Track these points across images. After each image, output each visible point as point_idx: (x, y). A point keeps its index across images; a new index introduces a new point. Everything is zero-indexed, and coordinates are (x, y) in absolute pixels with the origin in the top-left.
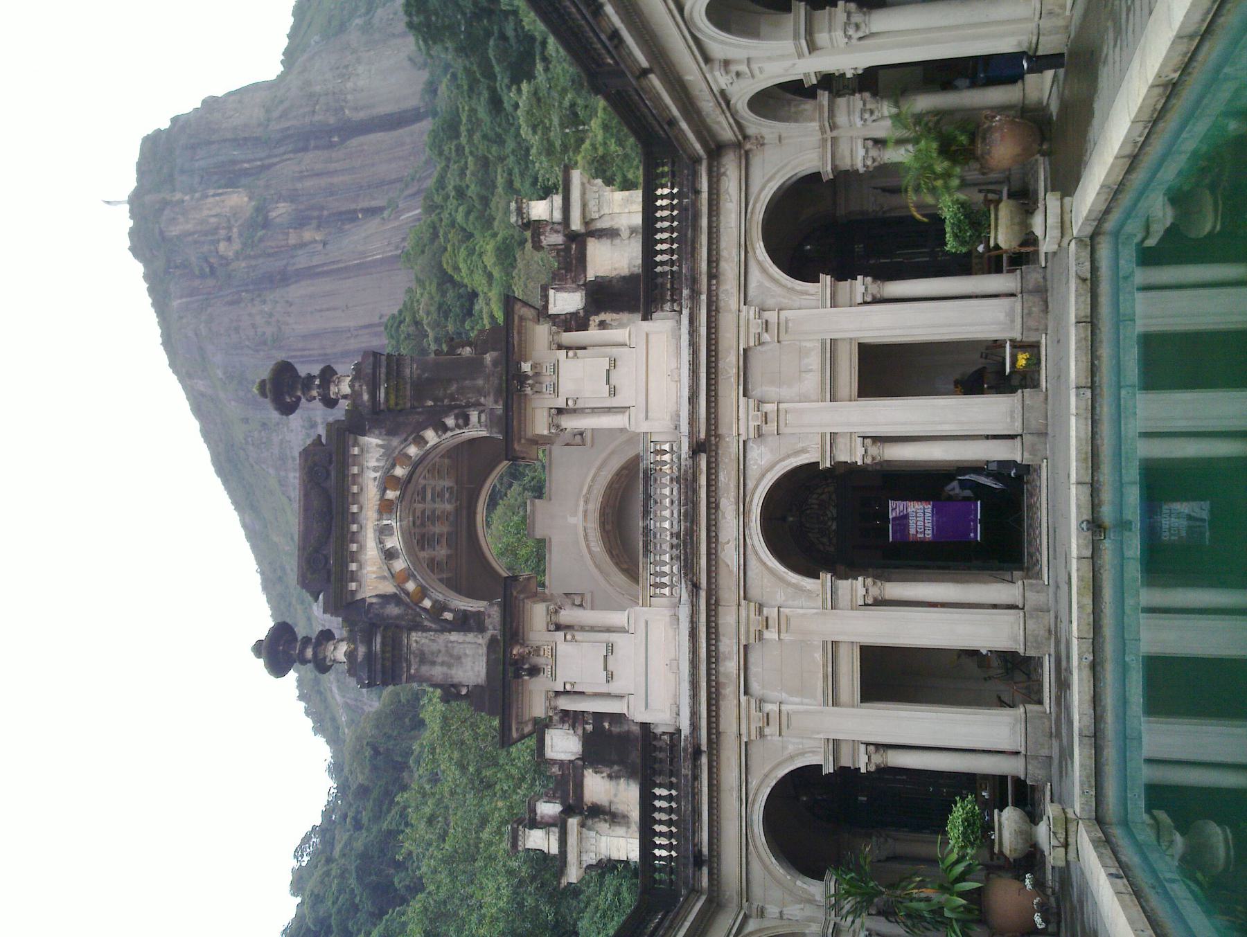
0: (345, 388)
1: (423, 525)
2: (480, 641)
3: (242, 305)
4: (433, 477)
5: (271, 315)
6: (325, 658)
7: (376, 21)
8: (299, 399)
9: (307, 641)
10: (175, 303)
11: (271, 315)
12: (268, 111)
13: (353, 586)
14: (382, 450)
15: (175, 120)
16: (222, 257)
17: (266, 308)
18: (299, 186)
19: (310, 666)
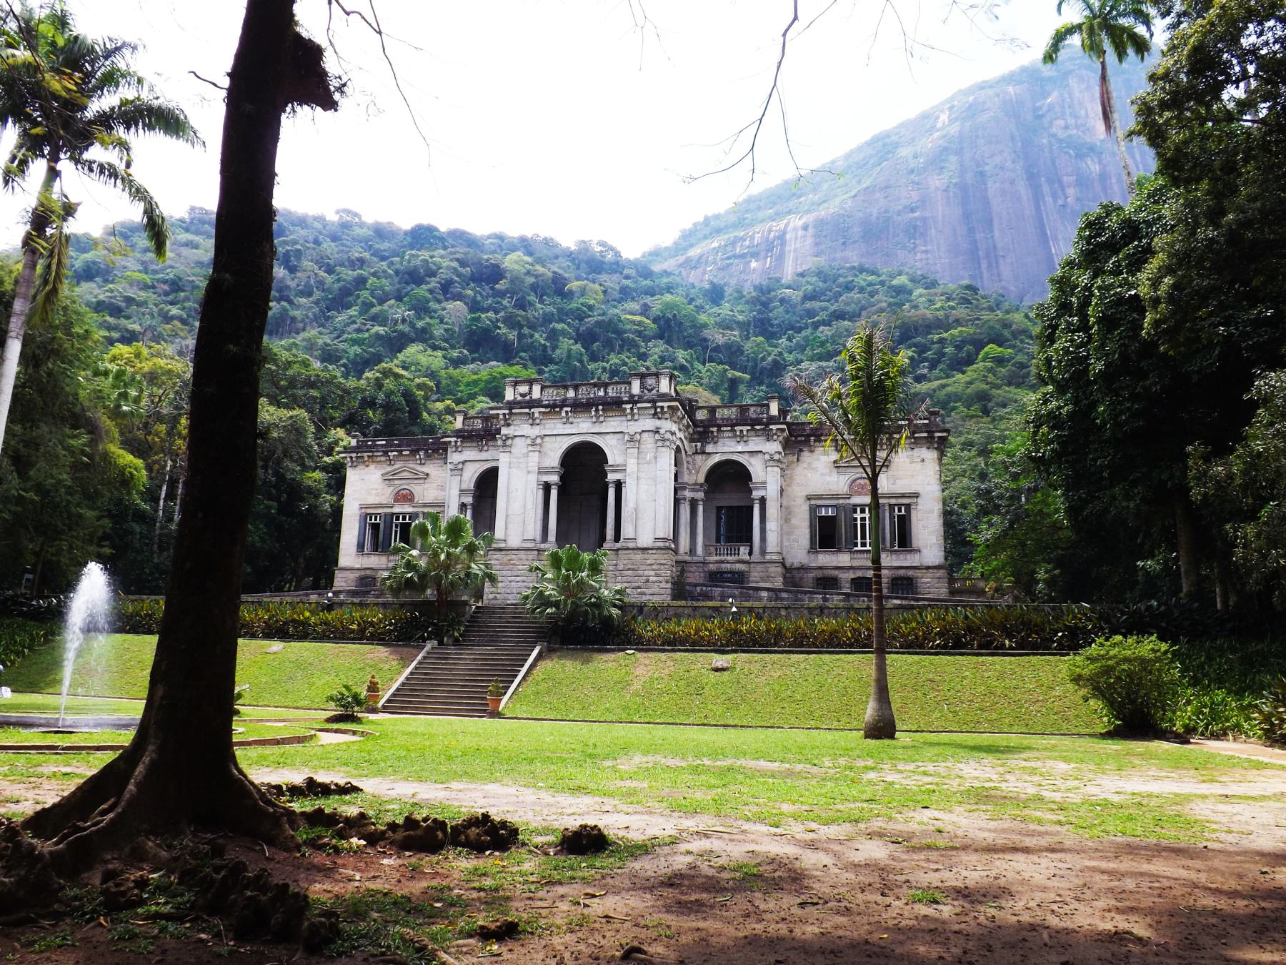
5: (1002, 168)
10: (1011, 89)
16: (1051, 123)
17: (1009, 164)
18: (1114, 180)
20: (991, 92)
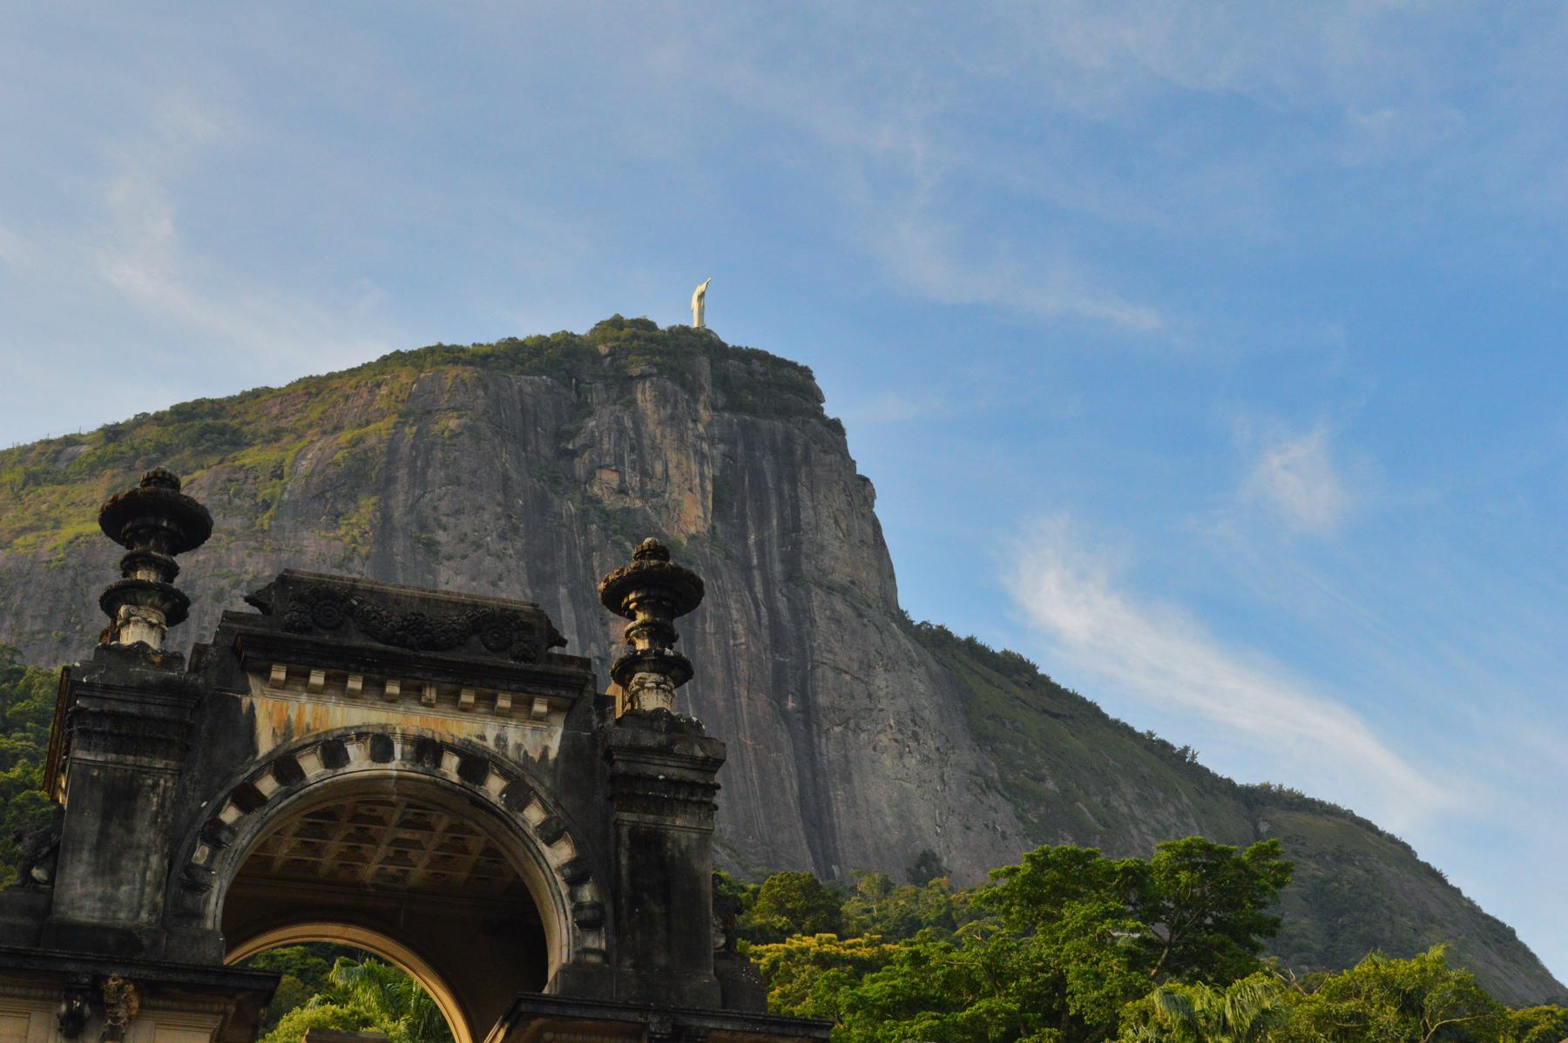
0: (651, 702)
1: (355, 818)
2: (144, 916)
3: (499, 497)
4: (441, 847)
5: (478, 545)
6: (136, 604)
7: (993, 799)
8: (632, 617)
9: (171, 571)
11: (478, 545)
12: (844, 591)
13: (279, 674)
14: (536, 756)
15: (836, 427)
16: (591, 475)
19: (114, 577)
20: (467, 373)
